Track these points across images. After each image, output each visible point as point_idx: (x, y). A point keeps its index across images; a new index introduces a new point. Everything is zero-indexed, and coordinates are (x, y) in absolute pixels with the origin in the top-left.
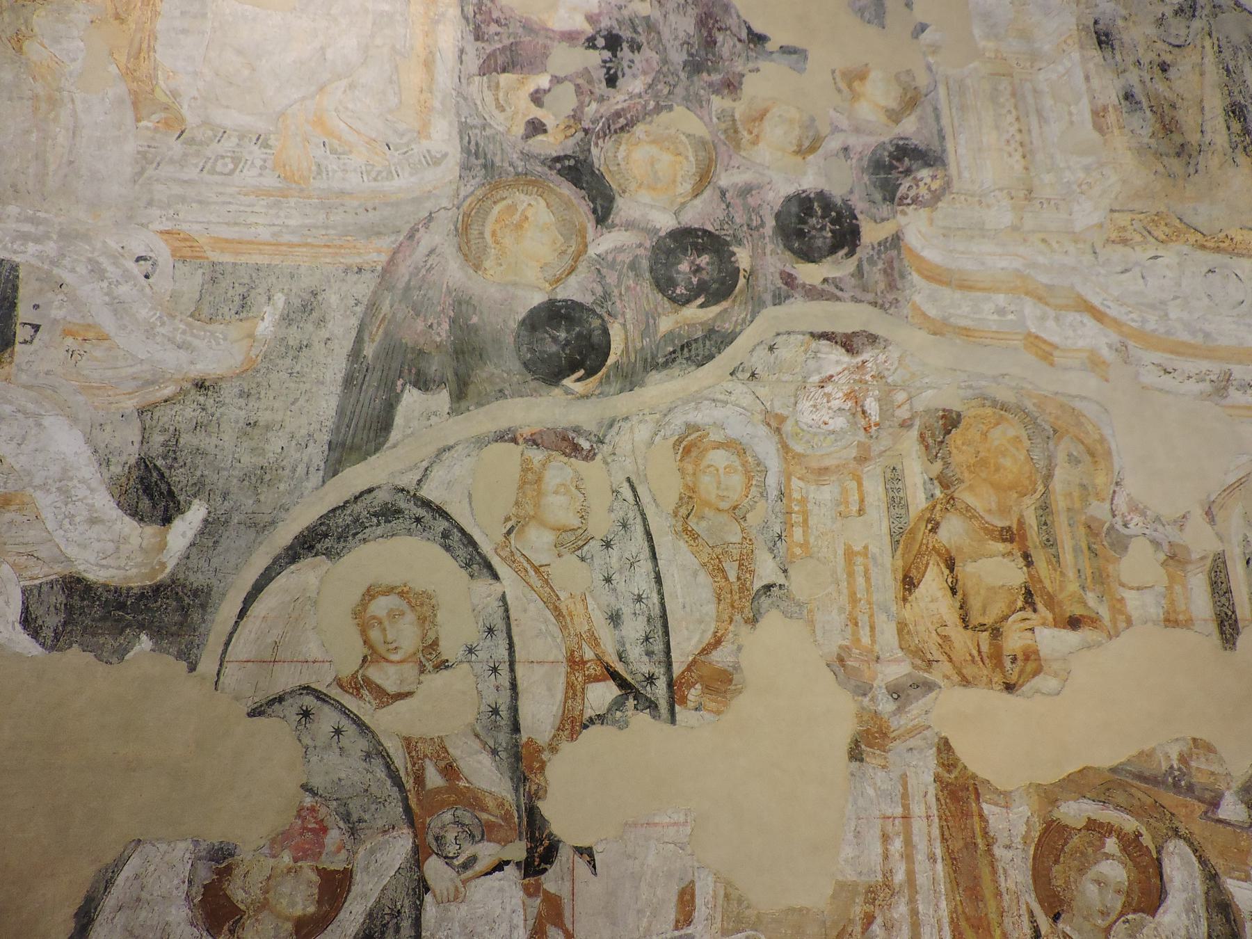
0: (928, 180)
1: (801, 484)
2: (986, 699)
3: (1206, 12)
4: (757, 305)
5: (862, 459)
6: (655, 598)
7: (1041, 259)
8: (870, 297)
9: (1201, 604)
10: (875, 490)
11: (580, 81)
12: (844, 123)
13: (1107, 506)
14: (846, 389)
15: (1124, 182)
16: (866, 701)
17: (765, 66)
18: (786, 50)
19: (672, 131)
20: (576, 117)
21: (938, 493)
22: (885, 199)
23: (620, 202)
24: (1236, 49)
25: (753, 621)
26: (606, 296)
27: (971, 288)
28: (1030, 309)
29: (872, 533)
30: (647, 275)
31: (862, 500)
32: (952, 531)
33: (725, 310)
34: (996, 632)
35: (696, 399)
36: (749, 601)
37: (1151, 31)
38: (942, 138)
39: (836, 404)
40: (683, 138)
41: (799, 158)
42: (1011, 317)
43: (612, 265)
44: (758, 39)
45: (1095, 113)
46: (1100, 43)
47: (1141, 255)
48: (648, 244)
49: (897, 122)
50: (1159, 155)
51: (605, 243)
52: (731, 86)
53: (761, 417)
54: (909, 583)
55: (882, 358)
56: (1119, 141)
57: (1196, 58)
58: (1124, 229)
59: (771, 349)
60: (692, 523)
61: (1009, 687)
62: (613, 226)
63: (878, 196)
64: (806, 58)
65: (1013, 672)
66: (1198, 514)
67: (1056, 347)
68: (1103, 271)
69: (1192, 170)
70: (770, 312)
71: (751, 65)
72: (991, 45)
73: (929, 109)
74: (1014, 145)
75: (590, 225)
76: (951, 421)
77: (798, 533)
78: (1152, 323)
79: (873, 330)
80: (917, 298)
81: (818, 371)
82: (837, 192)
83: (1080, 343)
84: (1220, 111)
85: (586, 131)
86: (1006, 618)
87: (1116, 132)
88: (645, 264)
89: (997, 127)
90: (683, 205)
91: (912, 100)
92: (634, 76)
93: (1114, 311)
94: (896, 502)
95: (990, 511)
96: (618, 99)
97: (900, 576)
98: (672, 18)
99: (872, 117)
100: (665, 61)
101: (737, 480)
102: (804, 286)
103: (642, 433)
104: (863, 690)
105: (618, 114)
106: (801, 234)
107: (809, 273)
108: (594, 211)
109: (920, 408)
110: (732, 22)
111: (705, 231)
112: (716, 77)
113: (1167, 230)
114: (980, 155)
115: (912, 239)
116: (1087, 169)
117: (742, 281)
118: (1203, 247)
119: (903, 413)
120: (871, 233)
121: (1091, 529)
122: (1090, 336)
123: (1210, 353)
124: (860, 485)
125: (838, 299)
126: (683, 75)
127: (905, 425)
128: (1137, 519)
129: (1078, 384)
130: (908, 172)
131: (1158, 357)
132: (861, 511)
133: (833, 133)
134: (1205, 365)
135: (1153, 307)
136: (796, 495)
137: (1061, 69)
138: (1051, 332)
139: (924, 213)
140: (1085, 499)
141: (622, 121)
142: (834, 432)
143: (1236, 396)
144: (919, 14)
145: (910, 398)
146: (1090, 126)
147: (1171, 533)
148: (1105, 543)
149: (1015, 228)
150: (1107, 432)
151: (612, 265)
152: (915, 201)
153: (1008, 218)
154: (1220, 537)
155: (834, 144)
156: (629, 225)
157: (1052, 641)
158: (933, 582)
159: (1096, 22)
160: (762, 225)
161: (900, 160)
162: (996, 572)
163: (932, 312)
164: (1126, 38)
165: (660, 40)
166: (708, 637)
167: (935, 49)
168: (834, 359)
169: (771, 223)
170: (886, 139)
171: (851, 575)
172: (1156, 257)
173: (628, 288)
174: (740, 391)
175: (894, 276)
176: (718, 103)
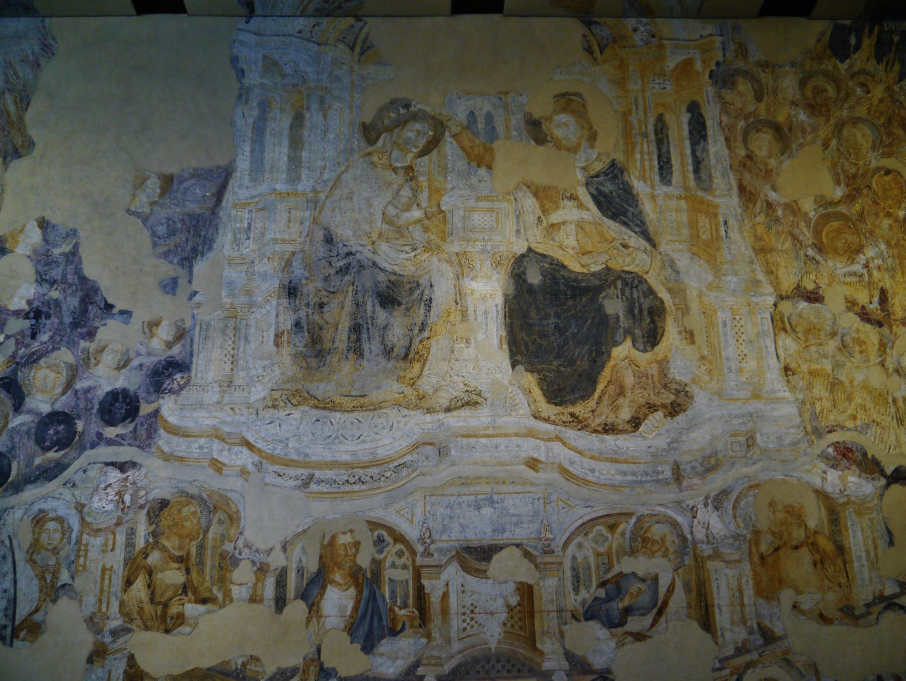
0: (179, 380)
1: (87, 537)
2: (156, 637)
3: (354, 270)
4: (82, 449)
5: (118, 524)
6: (12, 591)
7: (228, 419)
8: (137, 443)
9: (269, 590)
10: (121, 539)
11: (18, 337)
12: (143, 350)
13: (233, 544)
14: (116, 490)
15: (282, 373)
16: (99, 637)
17: (110, 322)
18: (122, 312)
19: (58, 361)
20: (14, 356)
21: (151, 540)
22: (155, 391)
23: (27, 400)
24: (366, 291)
25: (54, 601)
26: (13, 448)
27: (188, 436)
28: (216, 445)
29: (117, 560)
30: (33, 437)
31: (114, 544)
32: (155, 558)
33: (66, 453)
34: (166, 606)
35: (45, 498)
36: (53, 591)
37: (320, 284)
38: (192, 355)
39: (110, 498)
40: (62, 364)
41: (117, 372)
42: (206, 450)
43: (18, 433)
44: (109, 307)
45: (276, 336)
46: (290, 294)
47: (282, 413)
48: (36, 421)
49: (170, 348)
50: (305, 357)
51: (17, 421)
52: (91, 335)
53: (73, 505)
54: (129, 583)
55: (137, 474)
56: (286, 350)
57: (341, 299)
58: (276, 400)
59: (85, 471)
60: (34, 557)
61: (167, 631)
62: (22, 412)
63: (152, 390)
64: (131, 316)
65: (168, 622)
66: (278, 547)
67: (224, 465)
68: (259, 423)
69: (322, 364)
70: (88, 453)
71: (103, 322)
72: (229, 301)
73: (188, 340)
74: (229, 357)
75: (11, 413)
76: (164, 504)
77: (82, 560)
78: (279, 451)
79: (135, 460)
80: (160, 443)
81: (105, 482)
82: (132, 388)
83: (238, 462)
84: (347, 329)
85: (17, 363)
86: (171, 599)
87: (285, 345)
88: (33, 431)
89: (222, 348)
90: (56, 400)
91: (181, 335)
92: (45, 332)
93: (260, 445)
94: (130, 544)
95: (174, 548)
96: (35, 346)
97: (125, 580)
98: (69, 299)
99: (159, 345)
100: (61, 323)
101: (58, 536)
102: (106, 438)
103: (18, 514)
104: (99, 632)
105: (33, 354)
106: (110, 412)
107: (111, 432)
108: (14, 405)
109: (150, 497)
110: (98, 299)
111: (65, 413)
112: (84, 330)
113: (299, 399)
114: (209, 365)
115: (165, 412)
116: (264, 368)
117: (77, 437)
118: (317, 407)
119: (142, 501)
120: (145, 409)
121: (223, 556)
122: (245, 458)
123: (305, 465)
124: (115, 537)
125: (121, 445)
126: (68, 330)
127: (142, 507)
128: (246, 550)
129: (231, 484)
130: (170, 376)
131: (276, 468)
132: (113, 550)
133: (136, 357)
134: (300, 471)
135: (281, 441)
136: (84, 542)
137: (264, 311)
138: (224, 458)
139: (173, 397)
140: (222, 542)
141: (35, 357)
142: (106, 512)
143: (313, 487)
144: (194, 287)
145: (147, 494)
146: (272, 343)
147: (262, 557)
148: (228, 562)
149: (218, 403)
150: (241, 507)
151: (18, 433)
152: (170, 391)
153: (216, 398)
154: (287, 559)
155: (135, 363)
156: (30, 412)
157: (191, 609)
158: (140, 584)
159: (290, 282)
160: (92, 408)
161: (167, 369)
162: (173, 576)
163: (166, 449)
164: (305, 290)
165: (61, 312)
166: (33, 608)
167: (199, 305)
168: (114, 475)
169: (97, 406)
170: (162, 358)
171: (103, 579)
172: (289, 414)
173: (23, 444)
174: (67, 493)
175: (151, 432)
176: (83, 344)
